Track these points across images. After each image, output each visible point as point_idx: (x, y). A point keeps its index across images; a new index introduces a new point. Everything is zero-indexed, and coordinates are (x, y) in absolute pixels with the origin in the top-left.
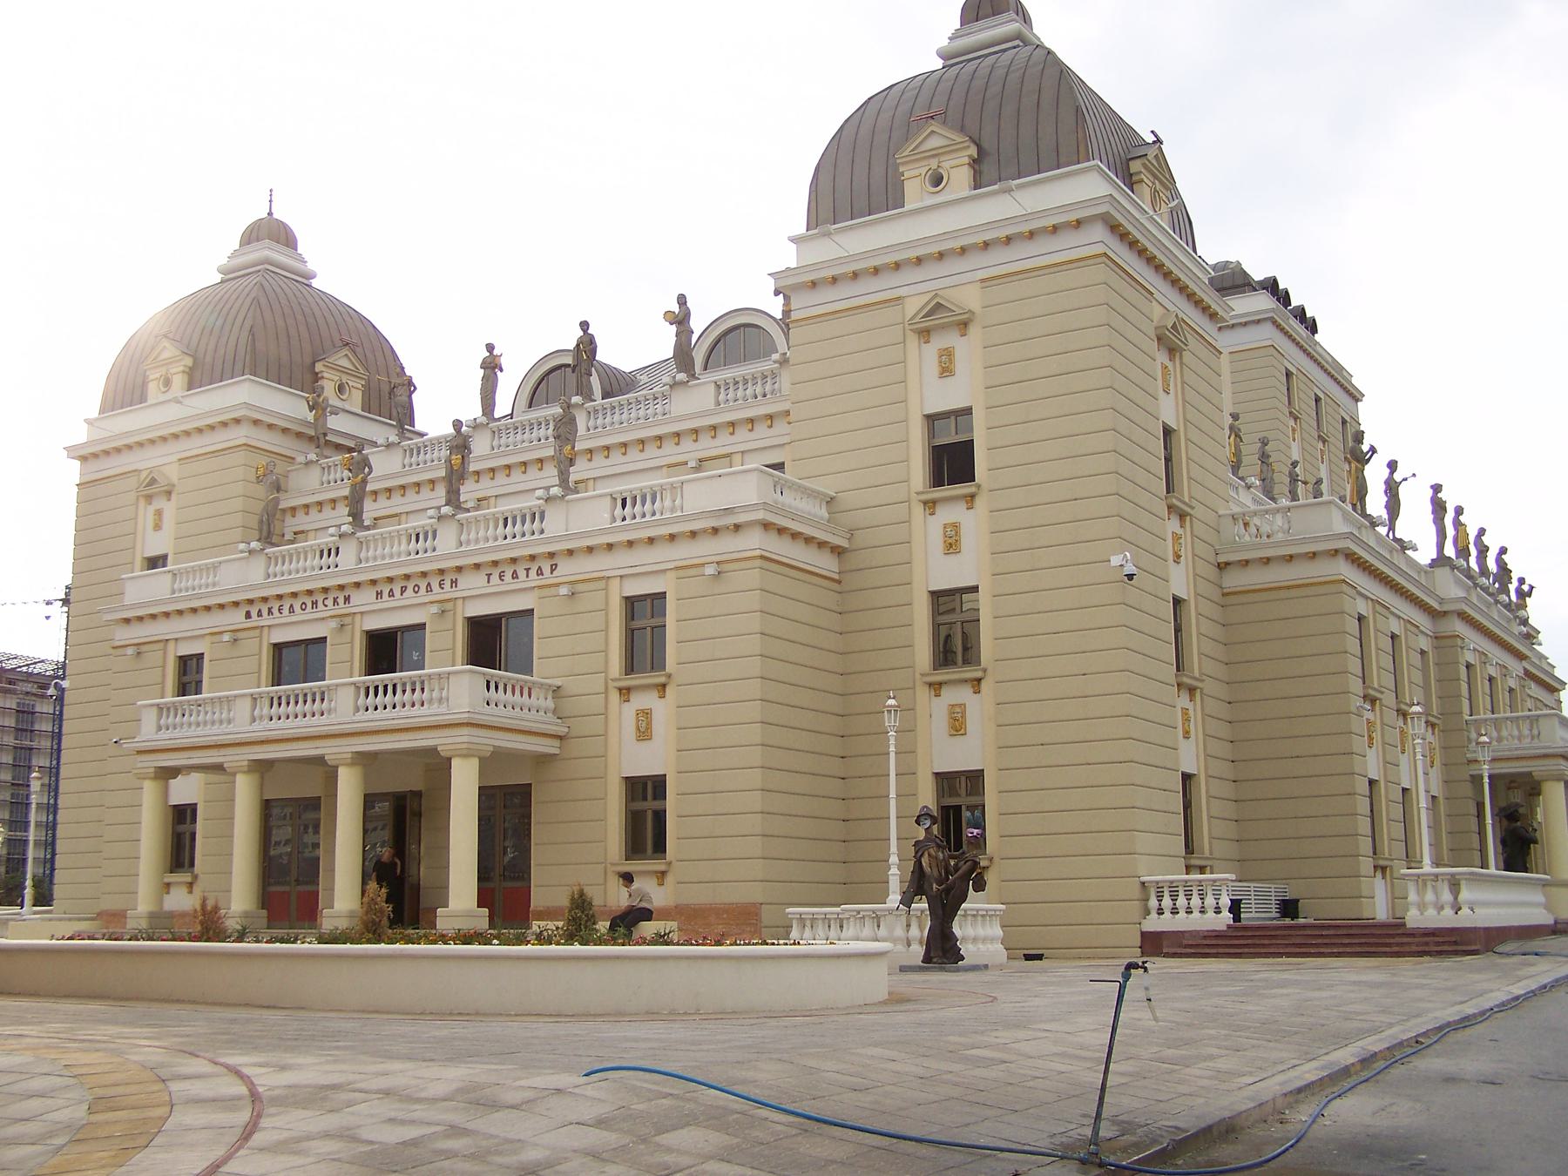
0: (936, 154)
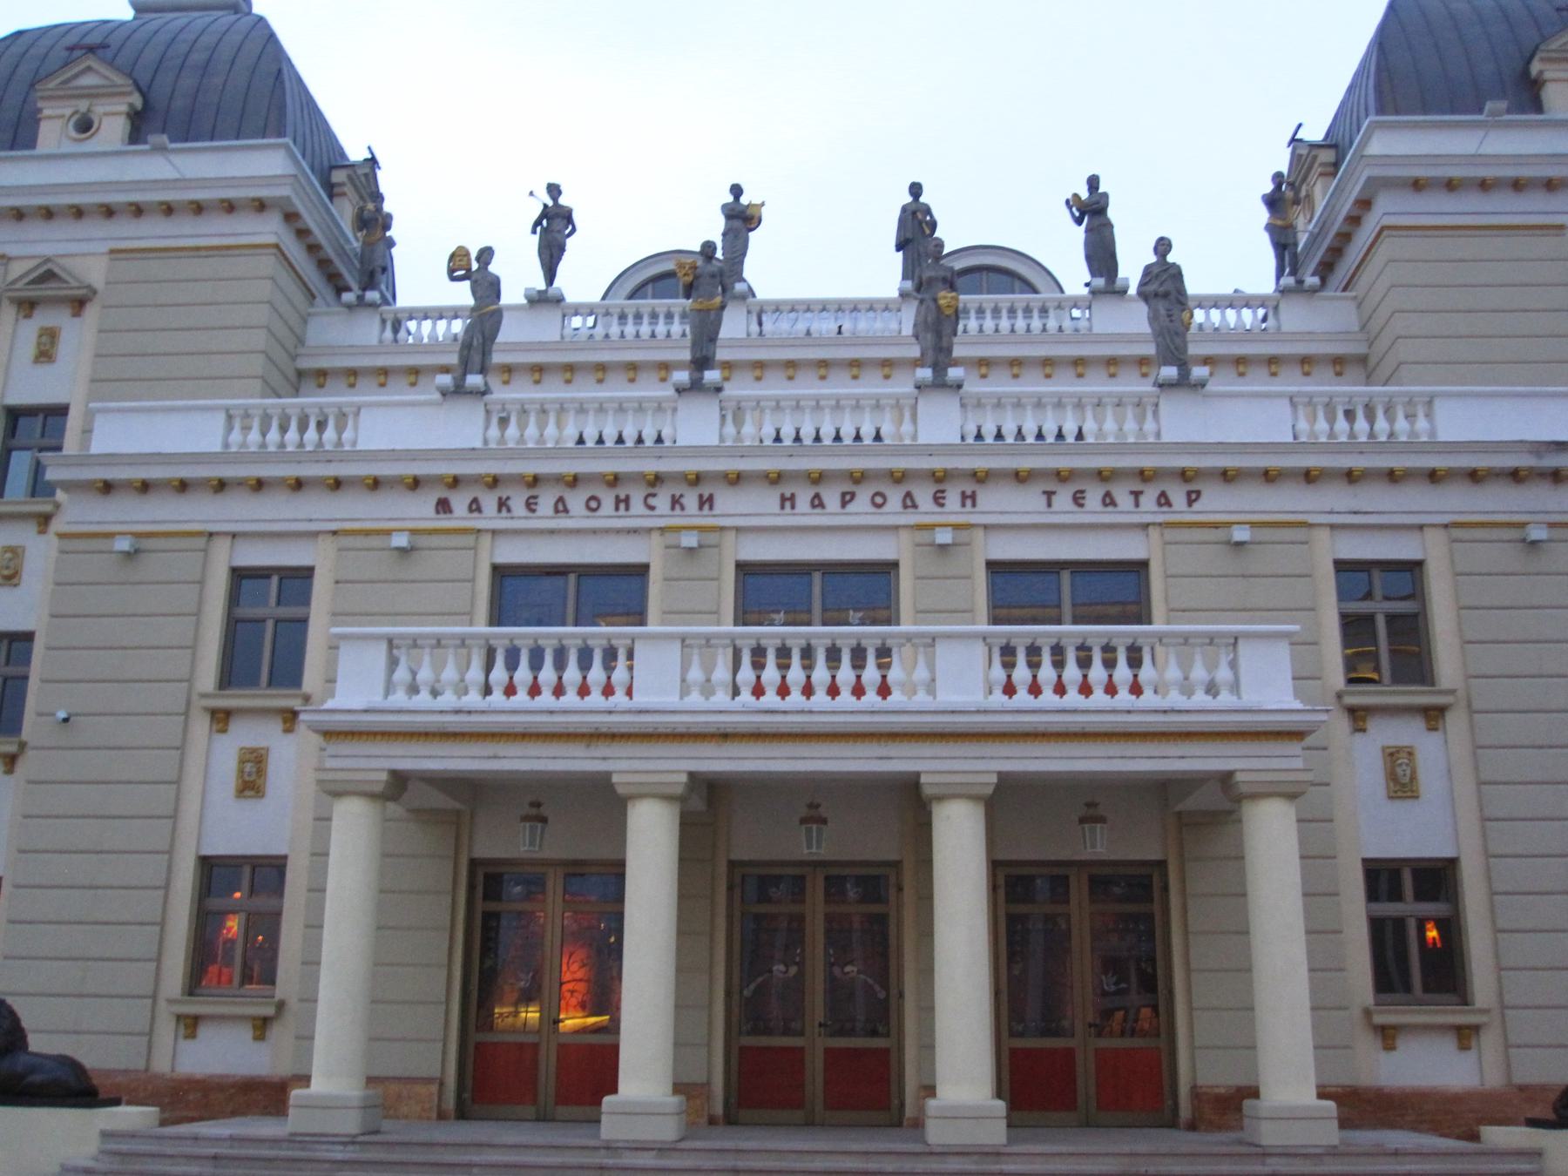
0: (92, 94)
